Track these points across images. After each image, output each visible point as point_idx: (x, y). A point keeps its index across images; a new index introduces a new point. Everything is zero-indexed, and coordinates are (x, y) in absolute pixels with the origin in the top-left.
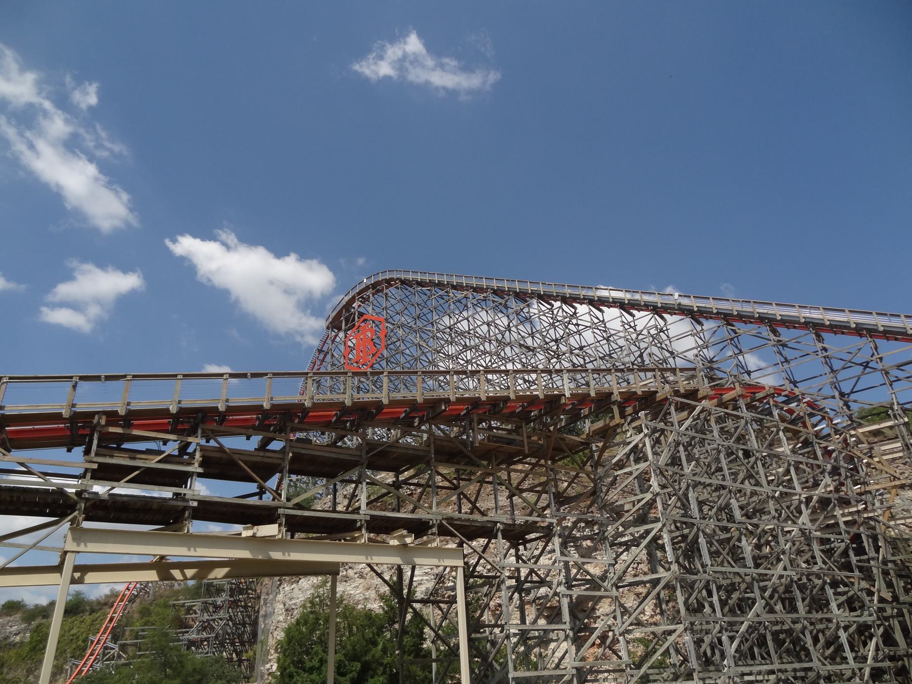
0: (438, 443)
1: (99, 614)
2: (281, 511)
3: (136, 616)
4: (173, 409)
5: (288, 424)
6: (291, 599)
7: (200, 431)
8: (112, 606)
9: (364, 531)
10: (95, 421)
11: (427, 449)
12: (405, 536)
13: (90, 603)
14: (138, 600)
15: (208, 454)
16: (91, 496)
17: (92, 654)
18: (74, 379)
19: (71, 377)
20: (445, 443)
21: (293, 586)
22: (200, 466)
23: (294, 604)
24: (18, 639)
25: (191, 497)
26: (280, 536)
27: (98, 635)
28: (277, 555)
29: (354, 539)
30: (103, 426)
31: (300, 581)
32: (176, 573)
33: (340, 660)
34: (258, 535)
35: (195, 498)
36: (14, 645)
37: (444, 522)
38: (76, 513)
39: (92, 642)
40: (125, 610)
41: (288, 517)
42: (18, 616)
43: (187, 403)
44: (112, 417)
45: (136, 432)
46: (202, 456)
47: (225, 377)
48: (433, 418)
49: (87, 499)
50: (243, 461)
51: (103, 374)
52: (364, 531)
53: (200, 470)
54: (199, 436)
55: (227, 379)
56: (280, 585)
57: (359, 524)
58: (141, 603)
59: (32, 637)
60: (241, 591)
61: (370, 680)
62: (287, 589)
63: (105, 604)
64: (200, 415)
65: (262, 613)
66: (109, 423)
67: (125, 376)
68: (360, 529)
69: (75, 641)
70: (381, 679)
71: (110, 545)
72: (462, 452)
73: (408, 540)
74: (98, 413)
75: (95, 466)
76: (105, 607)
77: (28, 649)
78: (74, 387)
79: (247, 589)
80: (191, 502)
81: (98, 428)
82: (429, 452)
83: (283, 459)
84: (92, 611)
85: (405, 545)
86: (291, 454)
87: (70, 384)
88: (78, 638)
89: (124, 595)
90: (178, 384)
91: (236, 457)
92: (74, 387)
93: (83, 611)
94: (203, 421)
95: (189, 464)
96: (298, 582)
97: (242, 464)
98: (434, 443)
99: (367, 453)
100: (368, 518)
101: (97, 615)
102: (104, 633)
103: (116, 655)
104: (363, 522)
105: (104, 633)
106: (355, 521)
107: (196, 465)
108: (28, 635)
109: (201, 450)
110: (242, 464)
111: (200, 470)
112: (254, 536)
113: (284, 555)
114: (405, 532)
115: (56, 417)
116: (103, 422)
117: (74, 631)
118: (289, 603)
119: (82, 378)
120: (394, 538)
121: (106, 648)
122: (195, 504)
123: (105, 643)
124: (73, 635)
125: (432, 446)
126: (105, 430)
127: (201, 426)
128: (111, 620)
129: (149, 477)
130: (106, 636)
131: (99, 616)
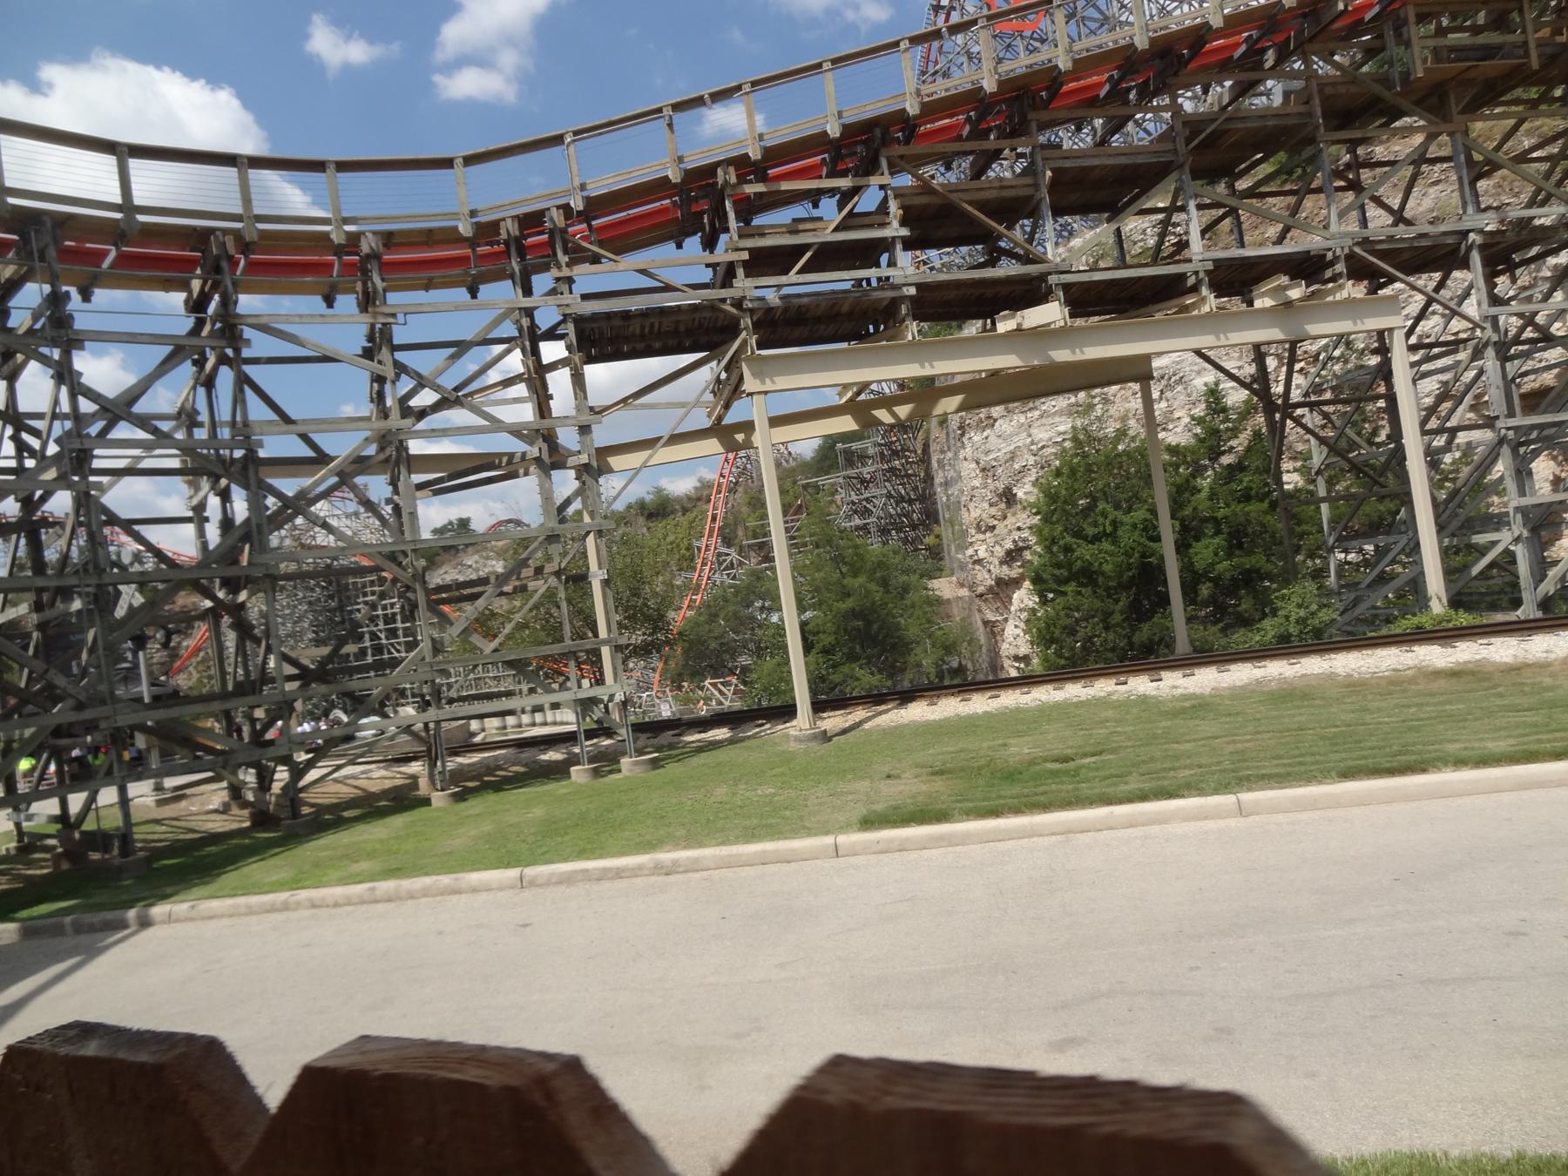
0: (1329, 91)
2: (1052, 279)
3: (745, 509)
4: (834, 130)
5: (1032, 115)
6: (987, 453)
7: (884, 163)
8: (709, 501)
9: (1205, 291)
10: (720, 180)
11: (1302, 109)
12: (1286, 288)
13: (678, 500)
14: (740, 489)
15: (908, 202)
16: (756, 304)
17: (704, 564)
18: (665, 112)
19: (659, 110)
20: (1342, 90)
21: (985, 434)
22: (903, 223)
23: (995, 459)
25: (902, 281)
26: (1062, 323)
27: (704, 540)
28: (1062, 355)
29: (1185, 309)
30: (734, 186)
31: (997, 424)
32: (883, 415)
33: (1146, 520)
34: (1025, 326)
35: (910, 280)
37: (1357, 250)
38: (744, 334)
39: (699, 549)
40: (727, 503)
41: (1067, 287)
43: (856, 114)
44: (741, 163)
45: (786, 186)
46: (902, 207)
47: (903, 46)
48: (1312, 39)
49: (752, 311)
50: (970, 203)
51: (705, 92)
52: (1205, 291)
53: (905, 232)
54: (886, 172)
55: (907, 50)
56: (963, 435)
57: (1191, 281)
58: (746, 492)
60: (895, 453)
61: (1194, 544)
62: (976, 439)
63: (699, 499)
64: (878, 132)
65: (938, 479)
66: (742, 179)
67: (739, 88)
68: (1195, 289)
69: (675, 550)
70: (1217, 540)
71: (806, 376)
72: (1377, 100)
73: (1295, 293)
74: (718, 164)
75: (745, 256)
76: (699, 504)
78: (670, 125)
79: (903, 450)
80: (905, 289)
81: (728, 191)
82: (1310, 115)
83: (1036, 186)
84: (685, 511)
85: (1289, 304)
86: (1049, 173)
87: (663, 123)
88: (678, 546)
89: (719, 485)
90: (829, 81)
91: (954, 197)
92: (670, 125)
93: (673, 512)
94: (887, 141)
95: (883, 225)
97: (970, 209)
98: (1321, 91)
99: (1188, 141)
100: (1210, 265)
101: (694, 515)
102: (710, 536)
104: (1202, 275)
105: (710, 536)
106: (1182, 277)
107: (895, 224)
109: (896, 197)
110: (970, 209)
111: (905, 232)
112: (1019, 329)
113: (1074, 353)
114: (1284, 280)
115: (660, 187)
116: (733, 179)
117: (671, 538)
118: (984, 459)
119: (677, 107)
120: (1263, 295)
121: (720, 555)
122: (912, 291)
125: (1317, 101)
126: (739, 190)
127: (884, 152)
128: (714, 519)
129: (829, 257)
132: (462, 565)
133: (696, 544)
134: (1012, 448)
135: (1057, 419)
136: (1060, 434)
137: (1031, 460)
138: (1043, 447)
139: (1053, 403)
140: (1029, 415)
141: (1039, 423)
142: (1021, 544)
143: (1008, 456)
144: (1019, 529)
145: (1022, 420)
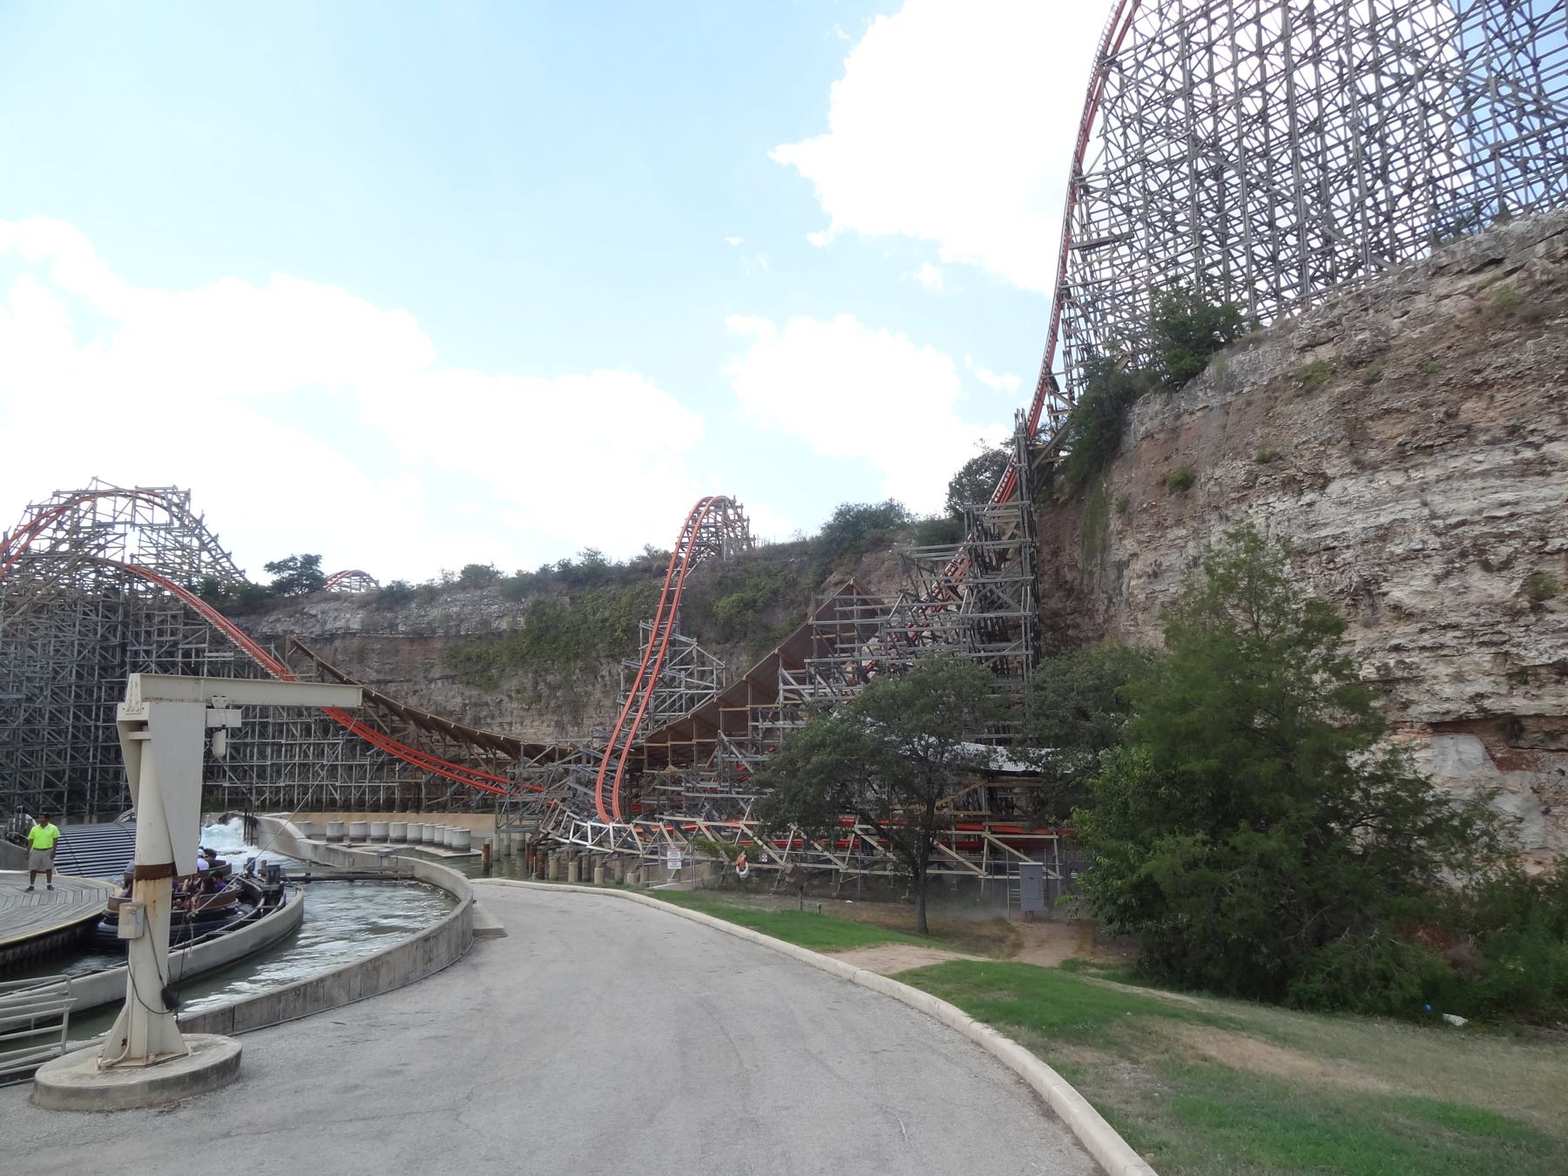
1: (638, 587)
6: (1311, 527)
21: (1307, 498)
23: (1335, 537)
24: (504, 625)
36: (500, 635)
42: (494, 590)
59: (528, 622)
77: (527, 642)
96: (1323, 487)
103: (695, 655)
108: (521, 620)
123: (670, 634)
124: (604, 621)
130: (670, 622)
131: (642, 591)
132: (302, 614)
133: (642, 625)
134: (1384, 519)
135: (1493, 482)
136: (1503, 505)
137: (1434, 542)
138: (1463, 523)
139: (1480, 457)
140: (1413, 474)
141: (1442, 486)
142: (1399, 674)
143: (1372, 534)
144: (1397, 648)
145: (1398, 479)
